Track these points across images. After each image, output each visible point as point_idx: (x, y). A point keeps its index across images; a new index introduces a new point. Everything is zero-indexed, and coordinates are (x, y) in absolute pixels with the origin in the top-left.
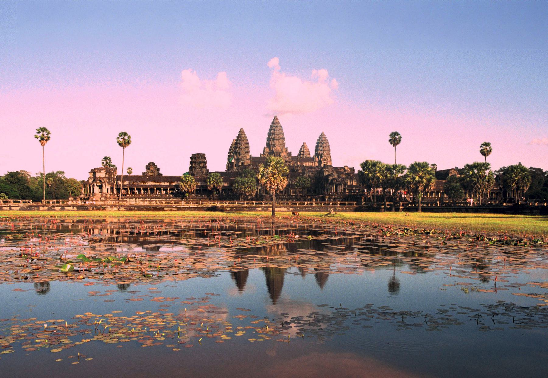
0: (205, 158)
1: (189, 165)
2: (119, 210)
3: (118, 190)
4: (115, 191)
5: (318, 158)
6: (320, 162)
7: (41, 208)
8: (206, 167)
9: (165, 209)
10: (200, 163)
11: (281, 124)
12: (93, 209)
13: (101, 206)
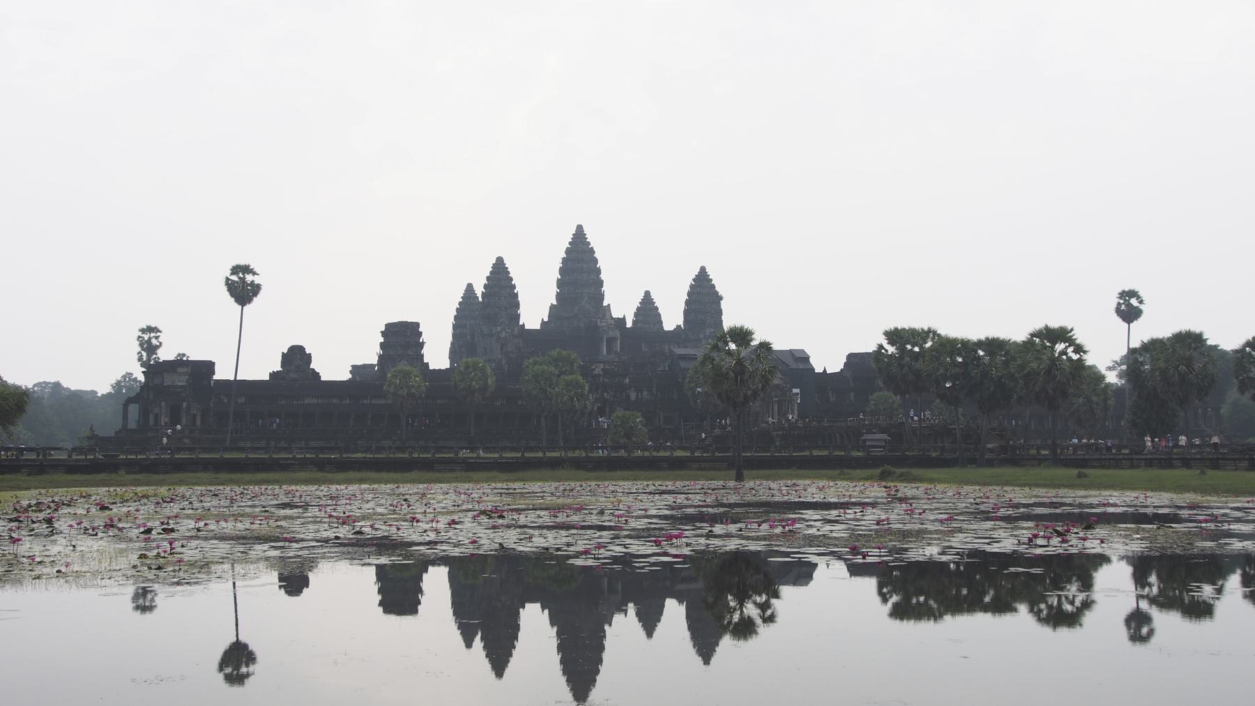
1: (378, 350)
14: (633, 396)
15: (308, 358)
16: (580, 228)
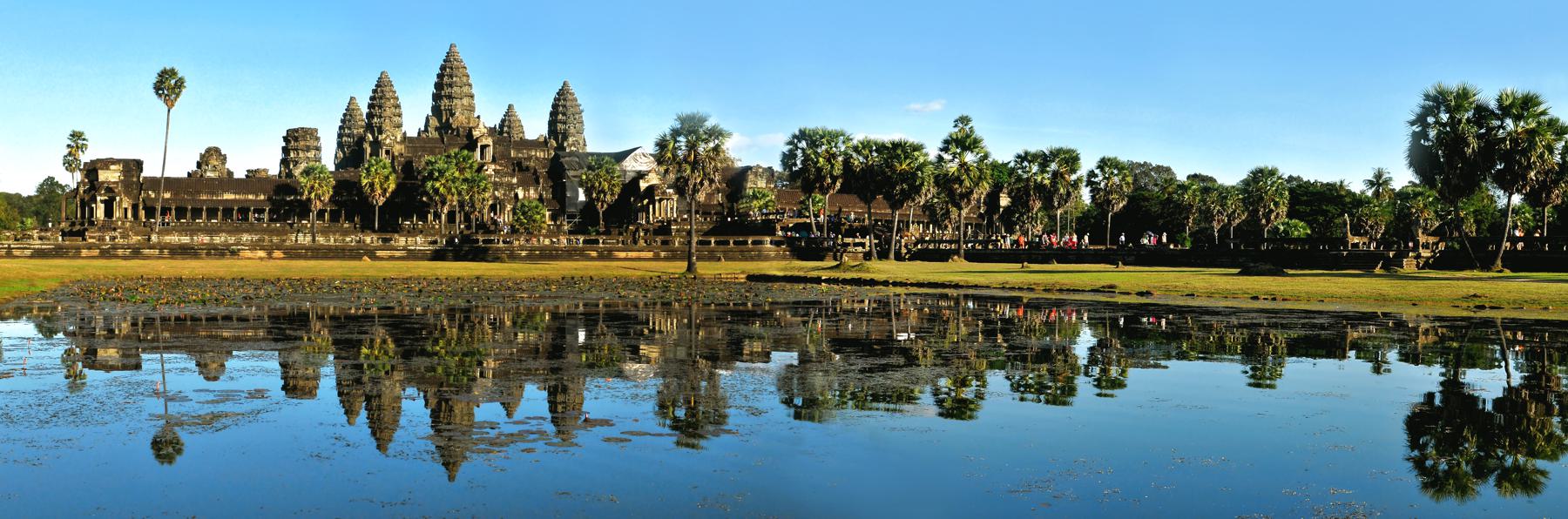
0: (318, 139)
1: (279, 155)
2: (270, 257)
3: (150, 212)
4: (142, 213)
5: (556, 139)
6: (561, 148)
7: (84, 252)
8: (319, 160)
9: (379, 253)
10: (308, 149)
11: (466, 62)
12: (208, 254)
13: (227, 246)
15: (224, 159)
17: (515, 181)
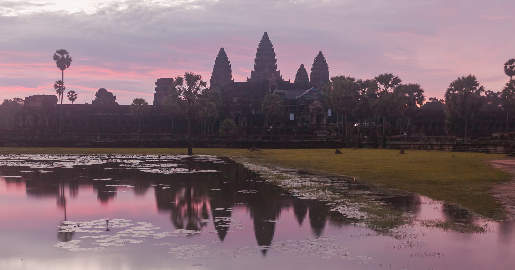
14: (253, 112)
16: (266, 34)
17: (251, 105)
